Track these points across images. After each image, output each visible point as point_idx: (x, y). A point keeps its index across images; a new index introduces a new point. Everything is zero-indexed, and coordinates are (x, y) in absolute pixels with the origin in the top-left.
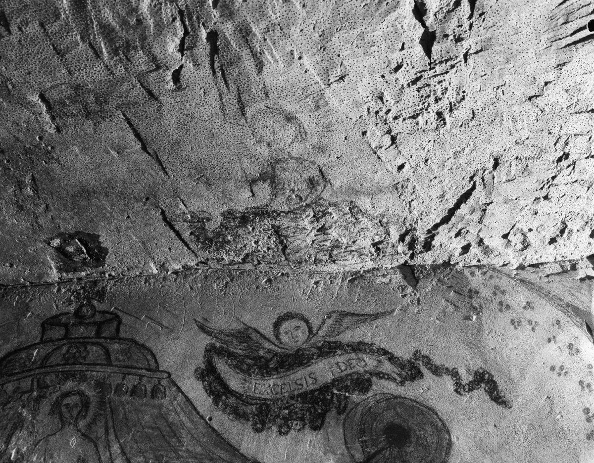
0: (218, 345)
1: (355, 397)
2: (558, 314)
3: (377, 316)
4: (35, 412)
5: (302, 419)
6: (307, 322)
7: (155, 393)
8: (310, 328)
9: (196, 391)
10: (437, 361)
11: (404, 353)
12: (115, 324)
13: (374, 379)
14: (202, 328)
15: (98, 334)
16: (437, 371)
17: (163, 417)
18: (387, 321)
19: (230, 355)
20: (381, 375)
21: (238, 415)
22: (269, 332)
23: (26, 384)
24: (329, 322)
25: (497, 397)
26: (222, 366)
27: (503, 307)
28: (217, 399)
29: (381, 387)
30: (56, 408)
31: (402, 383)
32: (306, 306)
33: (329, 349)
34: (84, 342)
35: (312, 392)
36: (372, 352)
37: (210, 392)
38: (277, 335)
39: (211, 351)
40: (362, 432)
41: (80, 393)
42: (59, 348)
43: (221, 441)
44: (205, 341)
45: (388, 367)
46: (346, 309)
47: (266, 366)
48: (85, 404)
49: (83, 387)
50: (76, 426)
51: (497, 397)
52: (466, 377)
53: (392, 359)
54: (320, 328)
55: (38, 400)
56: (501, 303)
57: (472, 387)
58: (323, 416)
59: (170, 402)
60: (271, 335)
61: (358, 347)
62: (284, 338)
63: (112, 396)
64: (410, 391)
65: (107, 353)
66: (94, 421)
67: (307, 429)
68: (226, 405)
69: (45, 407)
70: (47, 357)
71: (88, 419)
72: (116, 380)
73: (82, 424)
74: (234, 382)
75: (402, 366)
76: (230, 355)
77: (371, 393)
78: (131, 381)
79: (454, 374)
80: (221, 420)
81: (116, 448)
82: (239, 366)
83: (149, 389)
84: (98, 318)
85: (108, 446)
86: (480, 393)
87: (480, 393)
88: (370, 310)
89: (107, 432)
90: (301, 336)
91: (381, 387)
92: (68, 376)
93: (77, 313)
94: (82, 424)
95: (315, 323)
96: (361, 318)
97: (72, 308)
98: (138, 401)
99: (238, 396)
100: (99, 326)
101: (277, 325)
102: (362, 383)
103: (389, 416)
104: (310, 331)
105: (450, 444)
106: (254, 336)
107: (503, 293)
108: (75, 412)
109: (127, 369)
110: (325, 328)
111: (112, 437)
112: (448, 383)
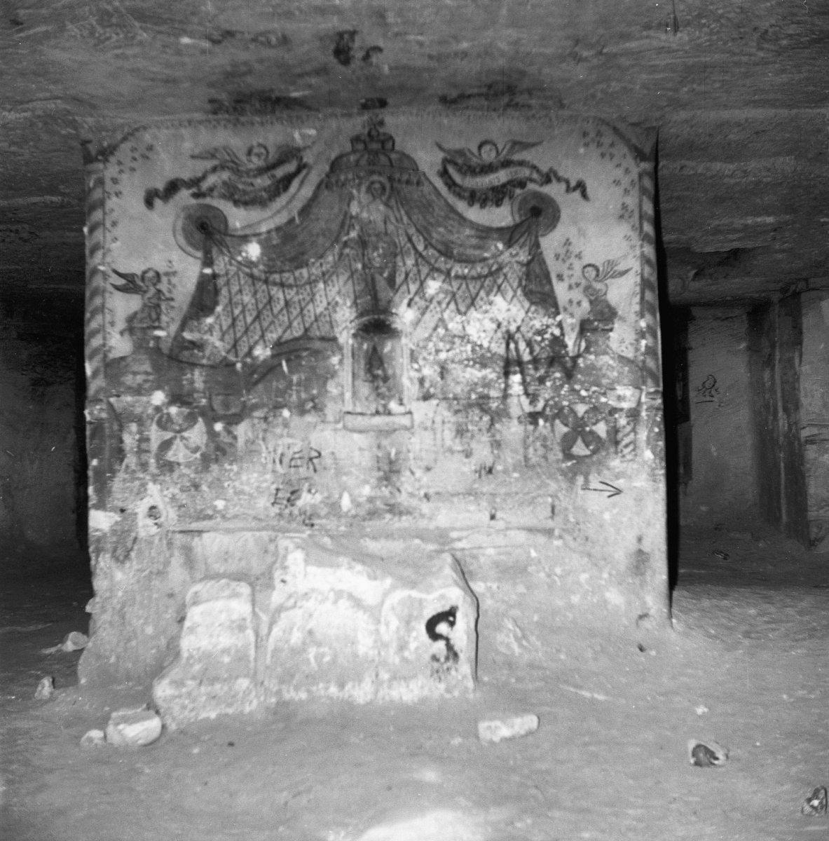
0: (449, 157)
1: (518, 191)
2: (625, 150)
3: (533, 145)
4: (359, 191)
5: (492, 200)
6: (495, 145)
7: (418, 183)
8: (497, 149)
9: (439, 183)
10: (561, 174)
11: (545, 169)
12: (391, 143)
13: (528, 183)
14: (440, 148)
15: (383, 147)
16: (559, 179)
17: (423, 196)
18: (540, 149)
19: (456, 164)
20: (532, 180)
21: (460, 196)
22: (475, 150)
23: (350, 176)
24: (508, 147)
25: (584, 195)
26: (451, 170)
27: (599, 145)
28: (450, 188)
29: (531, 187)
30: (369, 190)
31: (542, 185)
32: (494, 136)
33: (506, 164)
34: (376, 153)
35: (497, 187)
36: (528, 167)
37: (446, 184)
38: (480, 154)
39: (445, 161)
40: (520, 209)
41: (380, 182)
42: (362, 156)
43: (452, 209)
44: (441, 155)
45: (535, 176)
46: (518, 138)
47: (474, 171)
48: (384, 188)
49: (382, 179)
50: (381, 199)
51: (584, 195)
52: (573, 184)
53: (538, 171)
54: (503, 149)
55: (359, 185)
56: (598, 143)
57: (575, 189)
58: (502, 199)
59: (426, 189)
60: (477, 154)
61: (522, 163)
62: (484, 156)
63: (396, 185)
64: (547, 190)
65: (390, 160)
66: (389, 197)
67: (494, 206)
68: (454, 192)
69: (363, 189)
70: (358, 161)
71: (386, 197)
72: (397, 176)
73: (384, 198)
74: (457, 178)
75: (542, 176)
76: (456, 164)
77: (526, 189)
78: (405, 177)
79: (567, 182)
80: (452, 199)
81: (403, 212)
82: (459, 170)
83: (415, 181)
84: (382, 138)
85: (399, 211)
86: (577, 194)
87: (577, 194)
88: (531, 140)
89: (397, 203)
90: (493, 154)
91: (531, 187)
92: (372, 173)
93: (369, 134)
94: (384, 198)
95: (500, 147)
96: (526, 146)
97: (366, 131)
98: (409, 188)
99: (460, 187)
100: (383, 143)
101: (480, 147)
102: (522, 184)
103: (533, 203)
104: (497, 152)
105: (559, 217)
106: (468, 154)
107: (601, 136)
108: (379, 192)
109: (402, 170)
110: (506, 150)
111: (400, 206)
112: (563, 186)
